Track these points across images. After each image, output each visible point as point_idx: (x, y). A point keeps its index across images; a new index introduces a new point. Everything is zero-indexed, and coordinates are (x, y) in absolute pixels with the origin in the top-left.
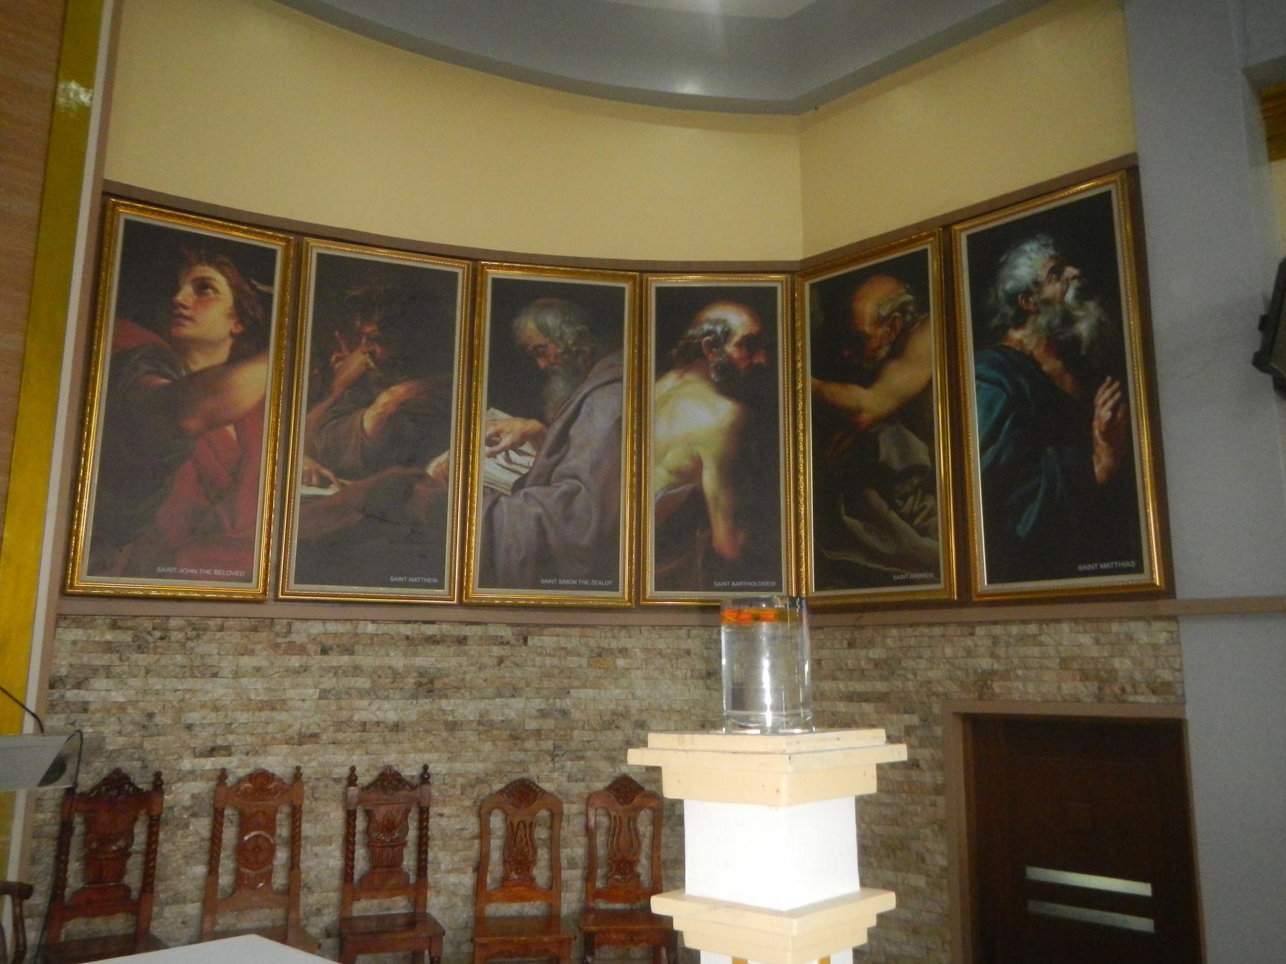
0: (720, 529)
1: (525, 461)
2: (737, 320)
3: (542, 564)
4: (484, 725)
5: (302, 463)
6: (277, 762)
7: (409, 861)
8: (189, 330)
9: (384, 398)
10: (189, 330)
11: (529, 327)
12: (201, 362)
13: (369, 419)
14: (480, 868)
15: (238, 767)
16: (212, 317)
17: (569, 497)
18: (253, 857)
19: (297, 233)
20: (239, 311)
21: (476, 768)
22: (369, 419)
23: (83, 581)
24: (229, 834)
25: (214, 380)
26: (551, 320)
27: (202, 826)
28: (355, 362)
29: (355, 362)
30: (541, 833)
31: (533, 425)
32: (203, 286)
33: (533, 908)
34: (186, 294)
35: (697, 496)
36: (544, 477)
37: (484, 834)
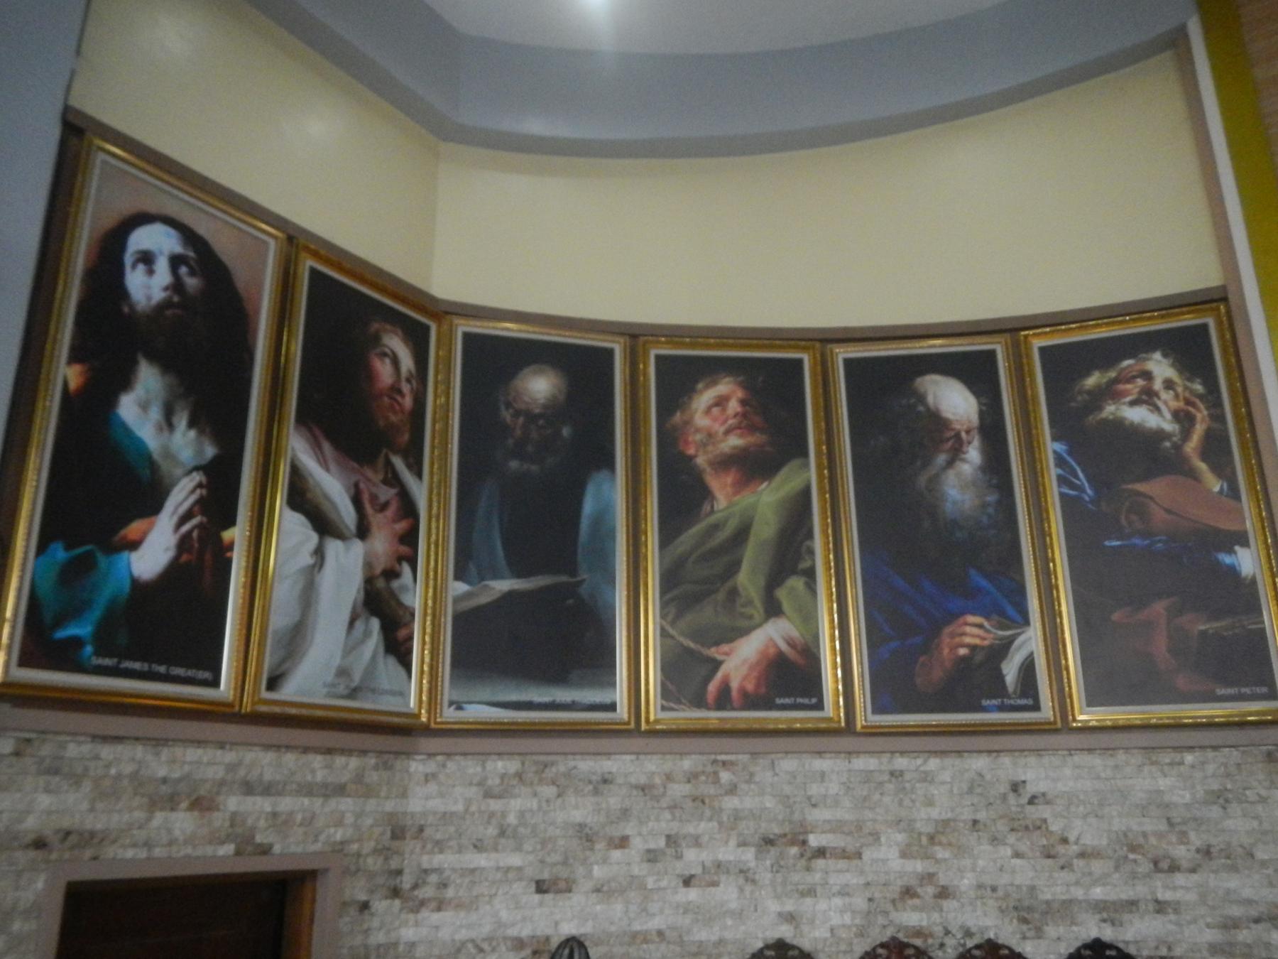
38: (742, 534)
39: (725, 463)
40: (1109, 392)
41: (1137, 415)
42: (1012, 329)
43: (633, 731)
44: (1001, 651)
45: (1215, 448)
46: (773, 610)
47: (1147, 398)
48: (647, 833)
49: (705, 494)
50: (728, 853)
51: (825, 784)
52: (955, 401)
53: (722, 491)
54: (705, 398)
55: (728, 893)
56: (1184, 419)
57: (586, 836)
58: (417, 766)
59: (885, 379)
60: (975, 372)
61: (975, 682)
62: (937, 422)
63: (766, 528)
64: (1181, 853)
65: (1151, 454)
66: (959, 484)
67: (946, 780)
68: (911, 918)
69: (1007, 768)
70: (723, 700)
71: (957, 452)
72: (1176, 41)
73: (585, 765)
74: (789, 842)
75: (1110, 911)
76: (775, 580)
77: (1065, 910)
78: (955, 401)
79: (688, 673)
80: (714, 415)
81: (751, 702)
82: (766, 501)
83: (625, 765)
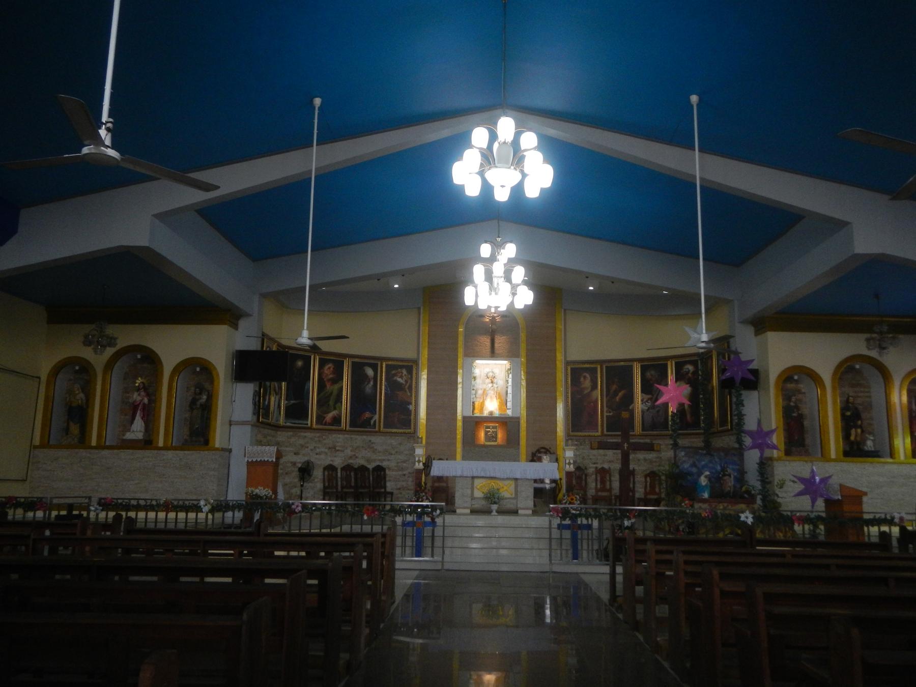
0: (689, 417)
1: (649, 404)
2: (690, 368)
3: (654, 426)
4: (645, 460)
5: (605, 409)
6: (606, 466)
7: (631, 486)
8: (583, 386)
9: (620, 394)
10: (583, 386)
11: (648, 374)
12: (586, 392)
13: (618, 398)
14: (646, 487)
15: (599, 466)
16: (587, 383)
17: (658, 411)
18: (603, 482)
19: (601, 362)
20: (592, 380)
21: (644, 468)
22: (618, 398)
23: (572, 434)
24: (599, 478)
25: (589, 395)
26: (653, 372)
27: (594, 476)
28: (614, 387)
29: (614, 387)
30: (657, 482)
31: (649, 396)
32: (585, 377)
33: (655, 497)
34: (582, 379)
35: (684, 409)
36: (653, 407)
37: (646, 482)
38: (331, 393)
39: (329, 380)
40: (395, 375)
41: (399, 380)
42: (382, 359)
43: (310, 429)
44: (371, 418)
45: (410, 388)
46: (335, 409)
47: (401, 377)
48: (311, 447)
49: (325, 386)
50: (323, 450)
51: (340, 439)
52: (370, 372)
53: (329, 387)
54: (327, 367)
55: (323, 456)
56: (406, 381)
57: (302, 446)
58: (279, 433)
59: (359, 365)
60: (374, 367)
61: (367, 423)
62: (366, 376)
63: (335, 393)
64: (393, 452)
65: (400, 387)
66: (368, 388)
67: (359, 440)
68: (351, 461)
69: (369, 438)
70: (325, 424)
71: (369, 382)
72: (419, 309)
73: (302, 434)
74: (333, 449)
75: (382, 461)
76: (336, 403)
77: (375, 460)
78: (370, 372)
79: (320, 419)
80: (329, 369)
81: (330, 424)
82: (336, 387)
83: (309, 434)
